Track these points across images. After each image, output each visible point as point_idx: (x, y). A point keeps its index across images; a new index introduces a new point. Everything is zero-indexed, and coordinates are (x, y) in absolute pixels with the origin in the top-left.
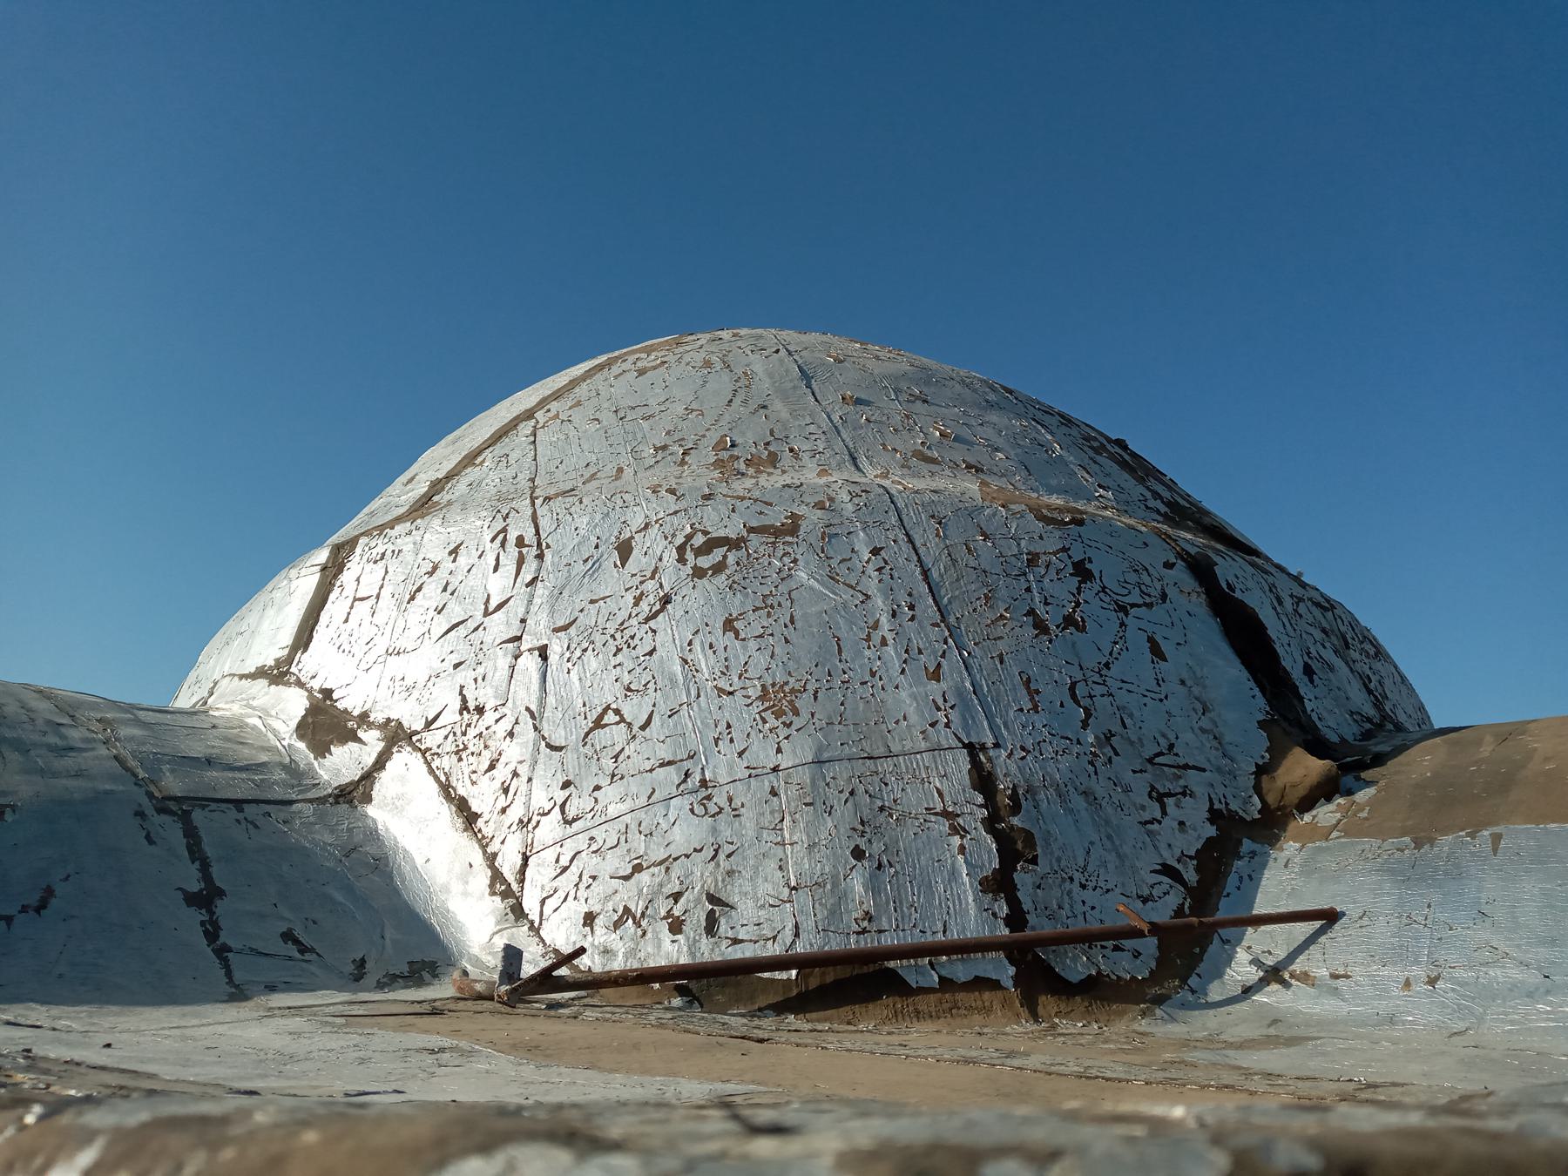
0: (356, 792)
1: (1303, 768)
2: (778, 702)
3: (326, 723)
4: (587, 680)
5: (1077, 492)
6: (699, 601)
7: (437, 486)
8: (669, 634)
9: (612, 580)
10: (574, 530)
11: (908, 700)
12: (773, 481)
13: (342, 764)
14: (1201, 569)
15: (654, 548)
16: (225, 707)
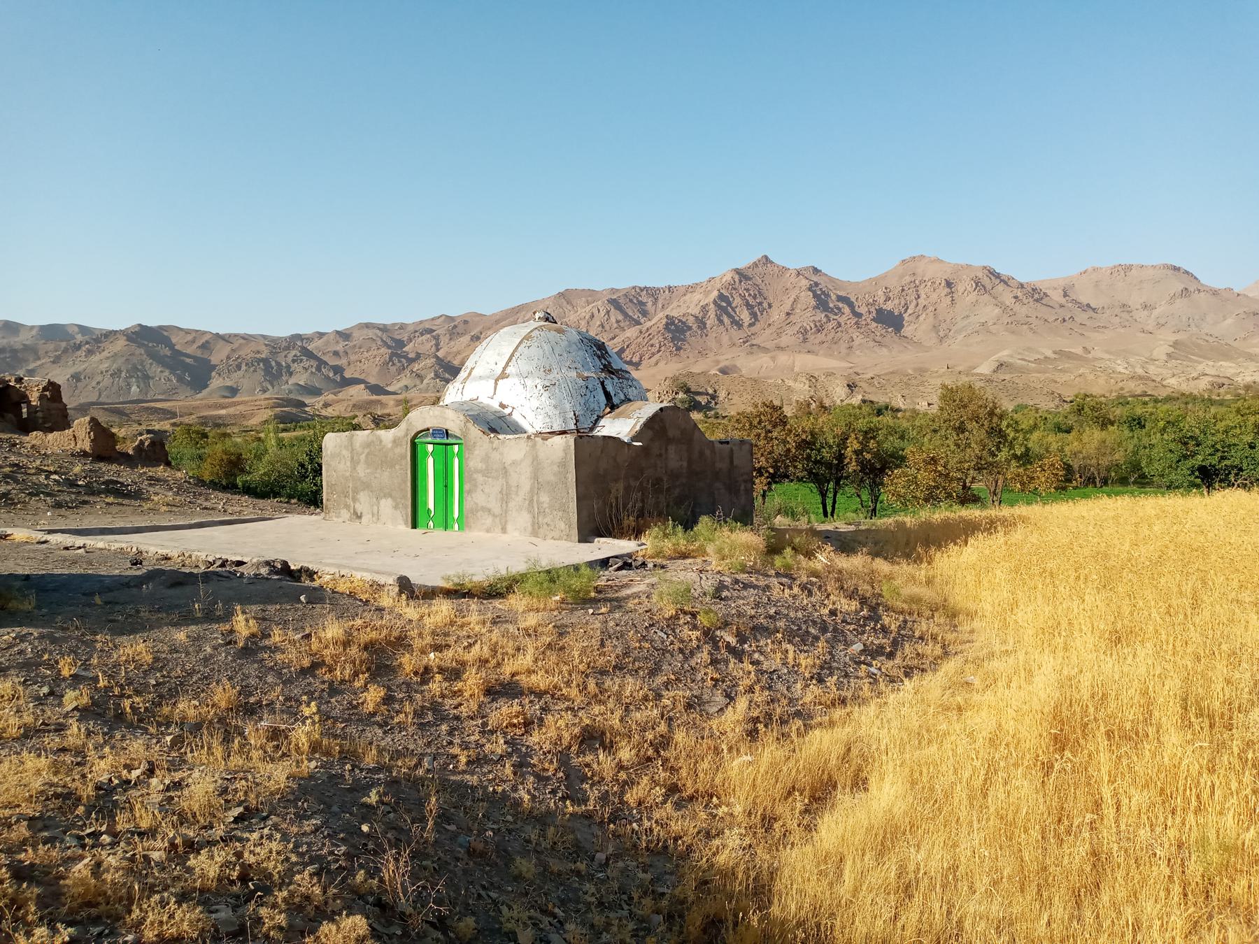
0: (510, 414)
1: (608, 410)
2: (555, 407)
3: (503, 406)
4: (535, 403)
5: (589, 370)
6: (546, 394)
7: (504, 369)
8: (543, 398)
9: (536, 391)
10: (529, 382)
11: (568, 406)
12: (550, 377)
13: (507, 411)
14: (602, 383)
15: (540, 387)
16: (484, 400)
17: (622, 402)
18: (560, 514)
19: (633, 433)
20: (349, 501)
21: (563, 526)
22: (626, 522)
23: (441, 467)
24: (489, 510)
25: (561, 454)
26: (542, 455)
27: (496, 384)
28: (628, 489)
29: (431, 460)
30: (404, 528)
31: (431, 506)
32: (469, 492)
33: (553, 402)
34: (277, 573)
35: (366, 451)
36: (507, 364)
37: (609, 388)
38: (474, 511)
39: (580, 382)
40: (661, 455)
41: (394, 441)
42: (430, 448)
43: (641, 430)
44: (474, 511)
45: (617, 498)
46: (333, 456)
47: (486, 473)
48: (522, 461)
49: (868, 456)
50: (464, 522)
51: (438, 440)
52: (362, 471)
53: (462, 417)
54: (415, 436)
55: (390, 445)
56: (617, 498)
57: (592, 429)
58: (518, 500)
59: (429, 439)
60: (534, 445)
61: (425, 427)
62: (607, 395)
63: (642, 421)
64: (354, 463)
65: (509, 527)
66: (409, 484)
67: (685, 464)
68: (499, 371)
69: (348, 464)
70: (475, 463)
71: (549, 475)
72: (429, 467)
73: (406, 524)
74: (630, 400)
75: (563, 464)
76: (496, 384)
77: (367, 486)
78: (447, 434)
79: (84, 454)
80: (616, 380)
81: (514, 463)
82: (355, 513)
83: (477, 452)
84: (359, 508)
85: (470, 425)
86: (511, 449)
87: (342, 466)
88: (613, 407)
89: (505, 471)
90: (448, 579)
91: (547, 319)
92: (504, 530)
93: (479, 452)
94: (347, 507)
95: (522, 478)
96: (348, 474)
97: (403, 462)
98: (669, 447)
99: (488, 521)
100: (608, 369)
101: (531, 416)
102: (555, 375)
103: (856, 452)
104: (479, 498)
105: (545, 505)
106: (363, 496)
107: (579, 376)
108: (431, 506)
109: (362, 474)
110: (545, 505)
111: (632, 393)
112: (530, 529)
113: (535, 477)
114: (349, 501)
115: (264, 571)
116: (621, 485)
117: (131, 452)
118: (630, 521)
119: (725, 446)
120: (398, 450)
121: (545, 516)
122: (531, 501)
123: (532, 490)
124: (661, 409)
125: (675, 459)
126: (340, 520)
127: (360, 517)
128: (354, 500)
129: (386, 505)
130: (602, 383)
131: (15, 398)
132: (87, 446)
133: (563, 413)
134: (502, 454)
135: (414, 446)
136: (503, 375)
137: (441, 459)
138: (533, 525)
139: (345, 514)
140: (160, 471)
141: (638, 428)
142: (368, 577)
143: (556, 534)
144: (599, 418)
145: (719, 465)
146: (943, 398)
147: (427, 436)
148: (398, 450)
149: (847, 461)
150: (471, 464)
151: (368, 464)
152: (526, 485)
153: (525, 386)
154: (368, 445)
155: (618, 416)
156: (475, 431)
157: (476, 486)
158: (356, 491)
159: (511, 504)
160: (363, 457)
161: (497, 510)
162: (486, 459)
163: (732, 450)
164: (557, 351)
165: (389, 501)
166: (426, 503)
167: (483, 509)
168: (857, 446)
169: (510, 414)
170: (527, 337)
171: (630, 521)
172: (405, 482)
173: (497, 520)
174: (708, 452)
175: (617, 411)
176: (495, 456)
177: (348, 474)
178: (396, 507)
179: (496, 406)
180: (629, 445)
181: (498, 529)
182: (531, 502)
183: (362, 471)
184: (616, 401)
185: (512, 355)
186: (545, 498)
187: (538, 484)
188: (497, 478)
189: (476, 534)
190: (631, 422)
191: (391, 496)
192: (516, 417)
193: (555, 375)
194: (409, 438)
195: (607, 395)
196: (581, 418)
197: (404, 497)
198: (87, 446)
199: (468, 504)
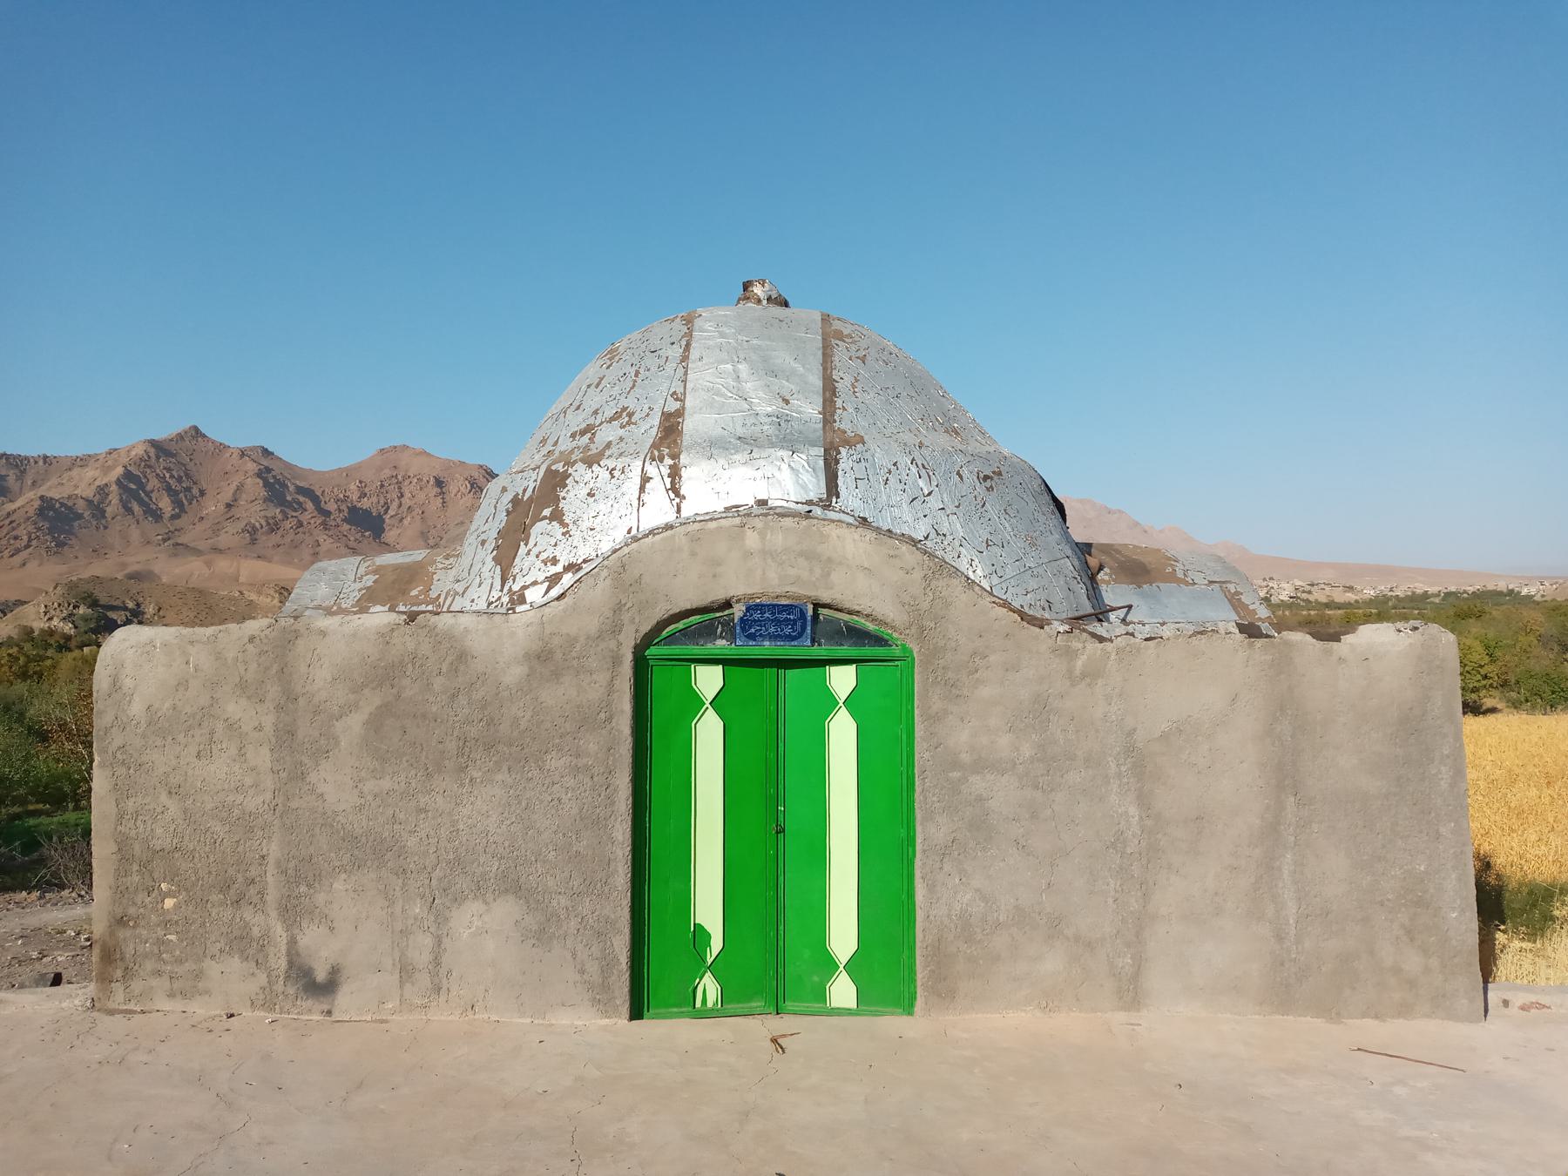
35: (372, 701)
51: (767, 649)
54: (648, 639)
59: (721, 646)
61: (719, 595)
64: (296, 744)
69: (262, 757)
73: (600, 999)
77: (374, 851)
87: (219, 769)
89: (1141, 767)
92: (1131, 993)
94: (245, 944)
97: (592, 744)
99: (1052, 963)
120: (557, 695)
126: (199, 1009)
129: (483, 929)
148: (557, 695)
160: (352, 727)
165: (505, 911)
166: (684, 902)
177: (253, 802)
178: (541, 936)
189: (995, 1024)
191: (512, 886)
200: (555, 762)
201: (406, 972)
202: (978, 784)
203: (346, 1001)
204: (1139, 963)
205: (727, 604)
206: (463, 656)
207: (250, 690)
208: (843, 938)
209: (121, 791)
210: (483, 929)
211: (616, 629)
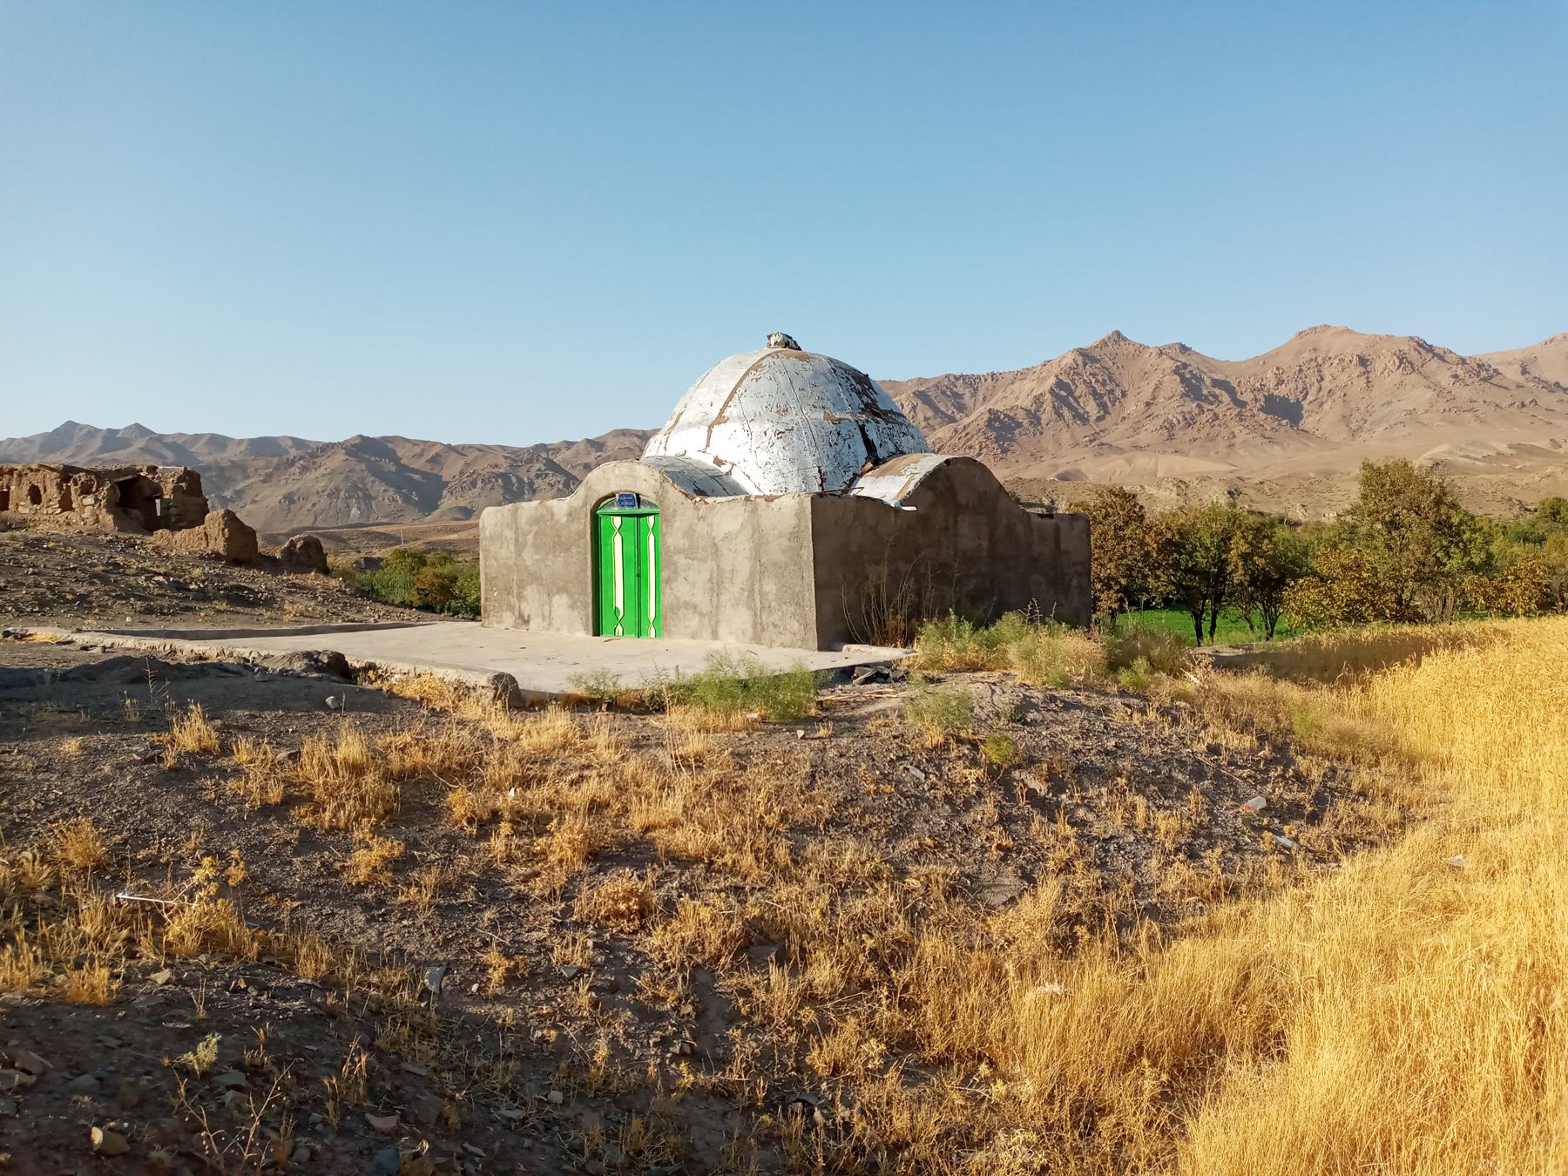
0: (729, 473)
1: (870, 465)
2: (792, 461)
3: (718, 462)
4: (763, 457)
5: (843, 410)
6: (779, 444)
7: (722, 411)
8: (775, 449)
9: (765, 439)
10: (755, 427)
11: (810, 460)
12: (788, 418)
13: (724, 469)
14: (862, 429)
16: (694, 456)
17: (891, 455)
18: (792, 609)
19: (904, 495)
20: (514, 600)
21: (795, 625)
22: (891, 623)
23: (632, 549)
24: (695, 607)
25: (793, 521)
26: (765, 524)
27: (710, 431)
28: (895, 577)
29: (618, 538)
30: (583, 635)
31: (619, 604)
32: (668, 581)
33: (789, 454)
34: (318, 670)
35: (535, 529)
36: (726, 404)
37: (872, 435)
38: (674, 608)
39: (830, 426)
40: (946, 529)
41: (570, 514)
42: (617, 521)
43: (916, 490)
44: (674, 608)
45: (877, 588)
46: (492, 538)
47: (690, 553)
48: (739, 532)
49: (1260, 562)
50: (663, 628)
51: (627, 510)
52: (529, 557)
53: (657, 475)
55: (564, 520)
56: (877, 588)
57: (845, 491)
58: (734, 590)
59: (616, 509)
60: (755, 510)
62: (869, 444)
63: (918, 478)
64: (520, 546)
65: (722, 630)
66: (589, 573)
67: (985, 544)
68: (715, 413)
69: (512, 548)
70: (675, 539)
71: (776, 551)
72: (616, 548)
74: (902, 453)
75: (795, 536)
76: (710, 431)
77: (535, 579)
78: (638, 500)
79: (217, 557)
80: (883, 424)
81: (727, 537)
82: (521, 616)
83: (677, 524)
84: (527, 609)
85: (668, 485)
86: (725, 516)
88: (877, 462)
90: (578, 680)
91: (787, 345)
92: (715, 635)
93: (680, 524)
94: (511, 608)
95: (739, 561)
96: (511, 562)
98: (960, 518)
99: (694, 622)
100: (872, 410)
101: (757, 476)
102: (794, 417)
103: (1245, 557)
104: (681, 590)
105: (771, 597)
106: (530, 592)
107: (827, 417)
108: (619, 604)
109: (529, 562)
110: (771, 597)
111: (905, 443)
112: (750, 631)
113: (757, 557)
114: (514, 600)
115: (298, 666)
116: (884, 570)
117: (278, 556)
118: (895, 622)
119: (1047, 521)
121: (770, 614)
122: (752, 592)
123: (752, 576)
124: (947, 462)
125: (969, 535)
126: (503, 626)
127: (527, 622)
128: (520, 597)
129: (560, 602)
130: (862, 429)
131: (147, 492)
132: (219, 546)
133: (802, 470)
134: (711, 525)
135: (595, 520)
136: (721, 419)
137: (632, 539)
138: (754, 626)
139: (508, 618)
140: (312, 578)
141: (911, 487)
142: (451, 675)
143: (787, 639)
144: (856, 476)
145: (1037, 549)
146: (1366, 482)
147: (612, 504)
148: (575, 527)
149: (1230, 569)
150: (670, 541)
151: (537, 548)
152: (744, 568)
153: (750, 433)
154: (536, 521)
155: (883, 474)
156: (674, 494)
157: (676, 572)
158: (521, 586)
159: (724, 598)
160: (530, 537)
161: (705, 606)
162: (689, 533)
163: (1057, 529)
164: (798, 383)
166: (612, 599)
167: (687, 605)
168: (1244, 548)
169: (729, 473)
170: (756, 367)
171: (895, 622)
172: (584, 570)
173: (706, 621)
174: (1020, 528)
175: (883, 467)
176: (701, 528)
177: (511, 562)
178: (572, 607)
179: (708, 461)
180: (896, 510)
181: (707, 634)
182: (752, 593)
183: (529, 557)
184: (881, 453)
185: (734, 391)
186: (770, 587)
187: (760, 568)
188: (704, 560)
190: (903, 480)
191: (566, 591)
192: (737, 476)
193: (794, 417)
194: (589, 508)
195: (869, 444)
196: (829, 477)
197: (583, 592)
198: (219, 546)
199: (667, 599)
200: (574, 550)
201: (544, 618)
202: (676, 558)
203: (532, 625)
204: (717, 623)
205: (613, 495)
206: (552, 515)
207: (509, 526)
208: (652, 616)
209: (486, 559)
210: (560, 602)
211: (585, 504)
